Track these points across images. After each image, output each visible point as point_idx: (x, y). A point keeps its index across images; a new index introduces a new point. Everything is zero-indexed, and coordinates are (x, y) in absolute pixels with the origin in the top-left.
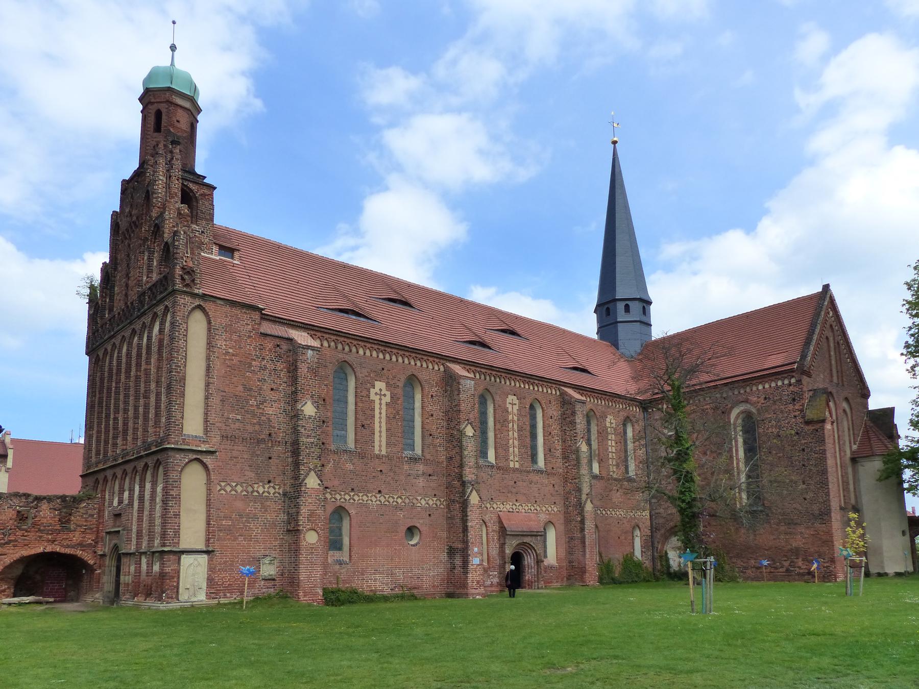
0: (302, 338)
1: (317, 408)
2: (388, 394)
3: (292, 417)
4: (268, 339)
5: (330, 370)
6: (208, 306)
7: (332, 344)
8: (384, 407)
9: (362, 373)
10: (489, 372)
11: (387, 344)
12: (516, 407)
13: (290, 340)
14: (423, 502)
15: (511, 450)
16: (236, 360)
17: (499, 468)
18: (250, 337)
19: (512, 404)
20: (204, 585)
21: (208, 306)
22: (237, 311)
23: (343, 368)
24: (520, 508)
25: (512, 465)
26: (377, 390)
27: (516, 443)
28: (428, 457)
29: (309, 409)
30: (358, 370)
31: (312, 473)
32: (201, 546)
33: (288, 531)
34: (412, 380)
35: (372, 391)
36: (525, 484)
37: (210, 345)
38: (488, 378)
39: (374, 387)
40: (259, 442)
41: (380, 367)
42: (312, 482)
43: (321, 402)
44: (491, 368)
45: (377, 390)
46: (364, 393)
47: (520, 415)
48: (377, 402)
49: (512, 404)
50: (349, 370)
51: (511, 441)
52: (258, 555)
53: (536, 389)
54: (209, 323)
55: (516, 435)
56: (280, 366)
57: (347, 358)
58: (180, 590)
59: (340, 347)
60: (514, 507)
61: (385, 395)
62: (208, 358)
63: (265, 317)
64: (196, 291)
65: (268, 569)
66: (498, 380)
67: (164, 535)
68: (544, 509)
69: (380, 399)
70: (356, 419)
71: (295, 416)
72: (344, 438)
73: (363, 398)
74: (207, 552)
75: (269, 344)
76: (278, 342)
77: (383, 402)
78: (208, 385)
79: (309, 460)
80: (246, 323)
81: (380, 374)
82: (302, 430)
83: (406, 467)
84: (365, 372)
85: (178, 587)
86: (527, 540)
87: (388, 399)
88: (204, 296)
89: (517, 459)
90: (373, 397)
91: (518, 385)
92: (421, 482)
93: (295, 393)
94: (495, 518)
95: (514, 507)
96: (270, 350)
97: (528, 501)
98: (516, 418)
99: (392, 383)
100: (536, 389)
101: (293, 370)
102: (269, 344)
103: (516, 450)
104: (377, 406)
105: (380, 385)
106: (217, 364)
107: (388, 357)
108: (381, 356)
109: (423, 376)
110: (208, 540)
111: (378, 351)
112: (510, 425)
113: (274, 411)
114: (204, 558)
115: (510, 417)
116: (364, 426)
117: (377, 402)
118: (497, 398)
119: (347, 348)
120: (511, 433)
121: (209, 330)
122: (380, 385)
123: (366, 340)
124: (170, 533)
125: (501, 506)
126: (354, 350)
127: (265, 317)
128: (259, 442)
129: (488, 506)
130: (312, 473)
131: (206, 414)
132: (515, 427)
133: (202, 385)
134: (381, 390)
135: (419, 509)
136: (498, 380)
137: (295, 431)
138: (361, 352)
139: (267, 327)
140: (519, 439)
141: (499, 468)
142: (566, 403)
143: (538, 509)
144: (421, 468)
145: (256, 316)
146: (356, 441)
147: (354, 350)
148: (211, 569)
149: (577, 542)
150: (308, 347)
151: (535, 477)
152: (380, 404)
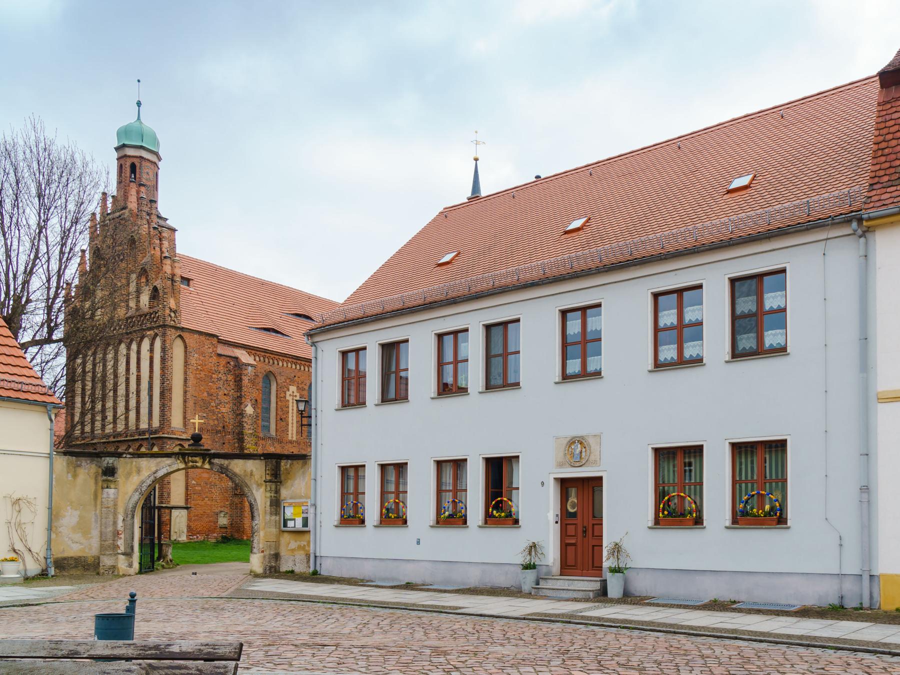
0: (245, 357)
1: (254, 408)
3: (237, 415)
4: (223, 358)
5: (260, 380)
6: (186, 335)
9: (281, 380)
11: (297, 358)
13: (237, 358)
16: (203, 374)
20: (185, 530)
21: (186, 335)
22: (203, 338)
23: (268, 377)
26: (290, 392)
29: (249, 410)
30: (278, 378)
32: (182, 504)
33: (236, 494)
37: (186, 363)
39: (288, 390)
40: (217, 432)
41: (293, 375)
43: (255, 405)
45: (290, 392)
46: (282, 395)
48: (291, 401)
50: (272, 378)
52: (217, 511)
54: (186, 347)
56: (230, 377)
57: (272, 369)
58: (172, 533)
59: (267, 360)
62: (185, 373)
65: (223, 521)
67: (161, 496)
70: (277, 414)
72: (268, 428)
73: (281, 398)
74: (187, 508)
75: (223, 361)
76: (228, 360)
78: (185, 392)
80: (207, 346)
81: (292, 381)
84: (283, 379)
85: (170, 531)
90: (288, 397)
93: (240, 397)
101: (238, 380)
102: (223, 361)
104: (291, 404)
105: (293, 388)
106: (191, 377)
107: (298, 367)
108: (294, 367)
110: (187, 500)
111: (292, 363)
113: (225, 409)
114: (184, 512)
116: (282, 420)
117: (291, 401)
119: (271, 361)
121: (186, 352)
123: (285, 355)
124: (165, 494)
126: (276, 362)
127: (221, 341)
128: (217, 432)
131: (185, 413)
133: (182, 393)
137: (240, 425)
139: (221, 350)
146: (277, 430)
147: (276, 362)
148: (189, 519)
150: (249, 365)
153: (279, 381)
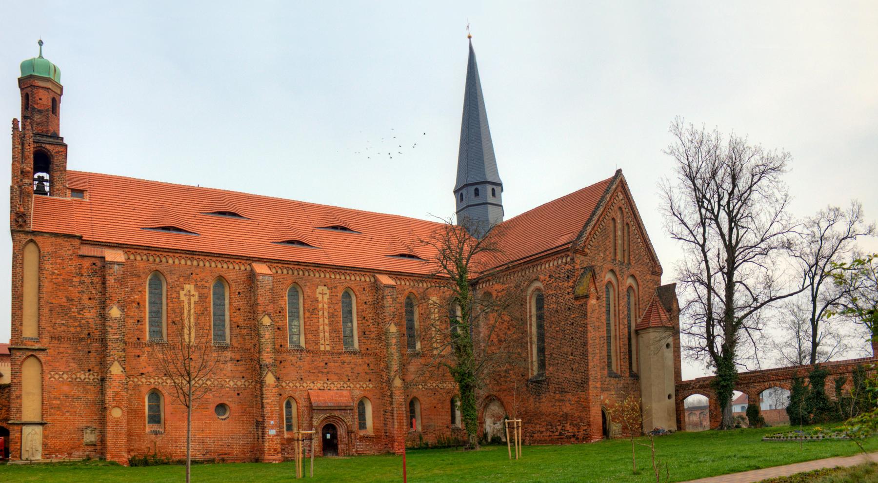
2: (197, 294)
4: (86, 259)
7: (145, 257)
8: (192, 306)
10: (297, 267)
12: (326, 297)
14: (232, 383)
15: (321, 335)
17: (308, 351)
18: (71, 259)
19: (323, 295)
24: (332, 386)
25: (322, 348)
26: (185, 291)
27: (327, 328)
28: (236, 345)
31: (116, 363)
34: (221, 281)
35: (182, 293)
36: (336, 364)
38: (296, 273)
39: (183, 289)
41: (189, 272)
42: (116, 370)
44: (299, 263)
46: (174, 295)
47: (331, 302)
49: (323, 295)
51: (321, 328)
53: (348, 278)
55: (326, 321)
56: (96, 279)
57: (159, 267)
59: (151, 259)
60: (325, 385)
61: (193, 295)
63: (84, 242)
64: (27, 229)
66: (307, 274)
68: (358, 386)
69: (189, 299)
70: (167, 317)
71: (104, 317)
77: (192, 301)
79: (115, 351)
81: (188, 278)
82: (109, 329)
83: (215, 354)
84: (175, 277)
86: (337, 413)
87: (196, 298)
88: (33, 233)
89: (327, 342)
90: (182, 297)
91: (328, 276)
92: (229, 367)
94: (305, 395)
95: (325, 385)
96: (88, 268)
97: (340, 379)
98: (326, 306)
99: (200, 284)
100: (348, 278)
103: (327, 335)
109: (230, 276)
112: (321, 313)
115: (320, 306)
118: (307, 290)
119: (158, 260)
120: (321, 320)
122: (189, 287)
123: (175, 251)
125: (312, 385)
126: (164, 260)
127: (84, 242)
129: (298, 385)
130: (116, 363)
132: (326, 314)
134: (189, 291)
135: (228, 389)
136: (307, 274)
138: (171, 261)
139: (86, 250)
140: (330, 324)
141: (308, 351)
142: (376, 287)
143: (352, 386)
144: (229, 354)
145: (77, 242)
149: (388, 414)
151: (347, 358)
152: (189, 304)
153: (170, 281)
